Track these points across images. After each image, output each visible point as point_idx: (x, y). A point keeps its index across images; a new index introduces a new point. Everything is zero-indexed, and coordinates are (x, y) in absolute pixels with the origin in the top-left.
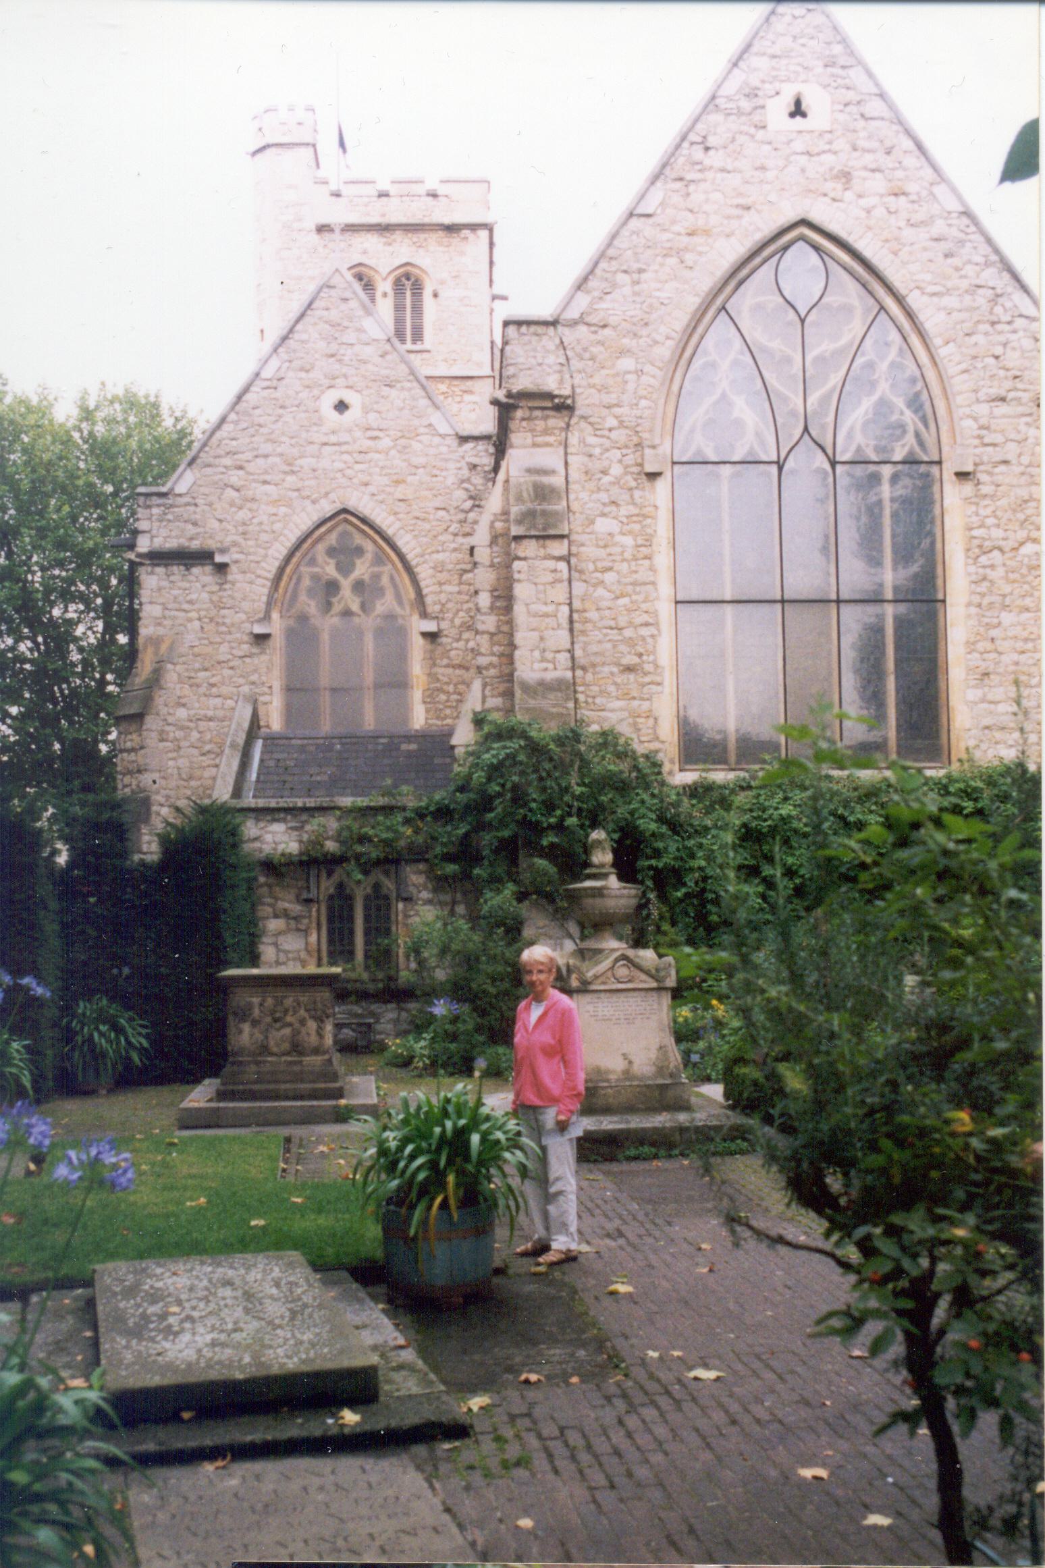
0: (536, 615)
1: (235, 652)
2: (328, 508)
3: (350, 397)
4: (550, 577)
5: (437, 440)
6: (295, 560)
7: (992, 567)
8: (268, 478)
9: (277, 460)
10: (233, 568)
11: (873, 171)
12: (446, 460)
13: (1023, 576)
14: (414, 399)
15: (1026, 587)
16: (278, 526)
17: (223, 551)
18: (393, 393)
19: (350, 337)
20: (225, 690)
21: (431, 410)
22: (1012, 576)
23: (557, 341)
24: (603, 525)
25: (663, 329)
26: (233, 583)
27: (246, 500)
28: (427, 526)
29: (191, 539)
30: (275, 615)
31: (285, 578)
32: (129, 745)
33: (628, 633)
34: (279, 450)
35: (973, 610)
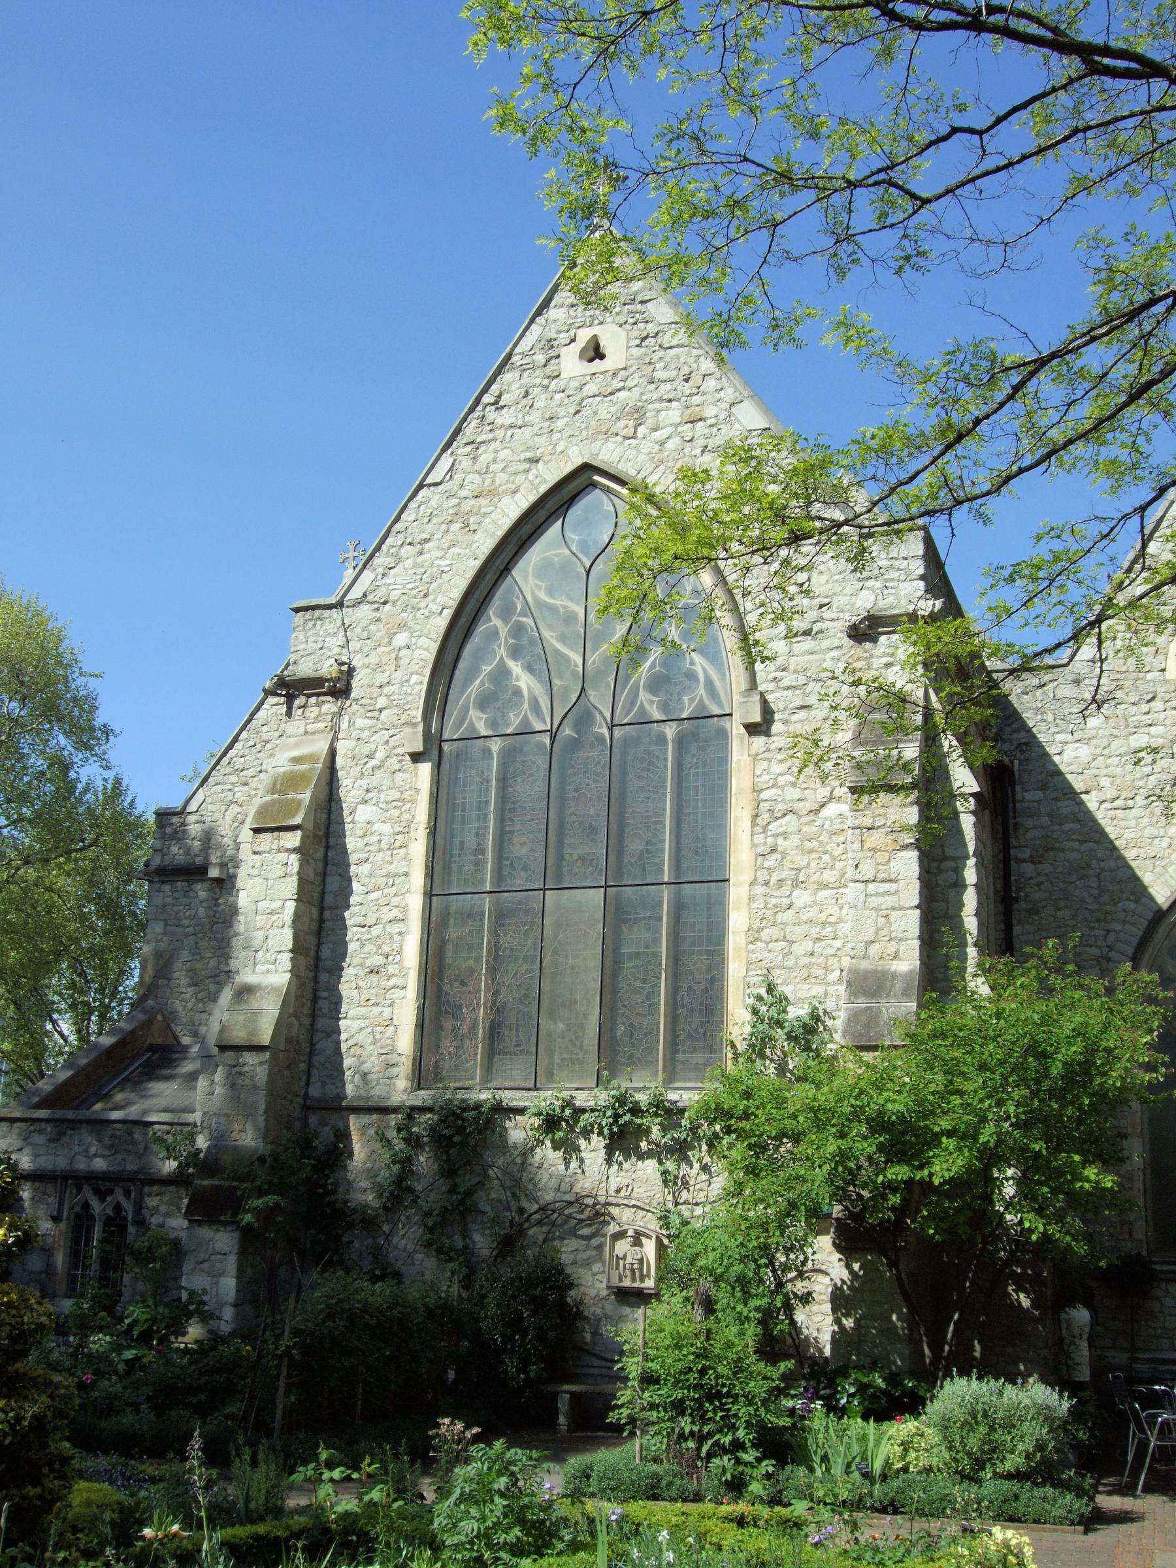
7: (785, 835)
11: (670, 401)
13: (821, 843)
15: (826, 857)
22: (808, 845)
23: (339, 623)
25: (441, 599)
35: (759, 889)
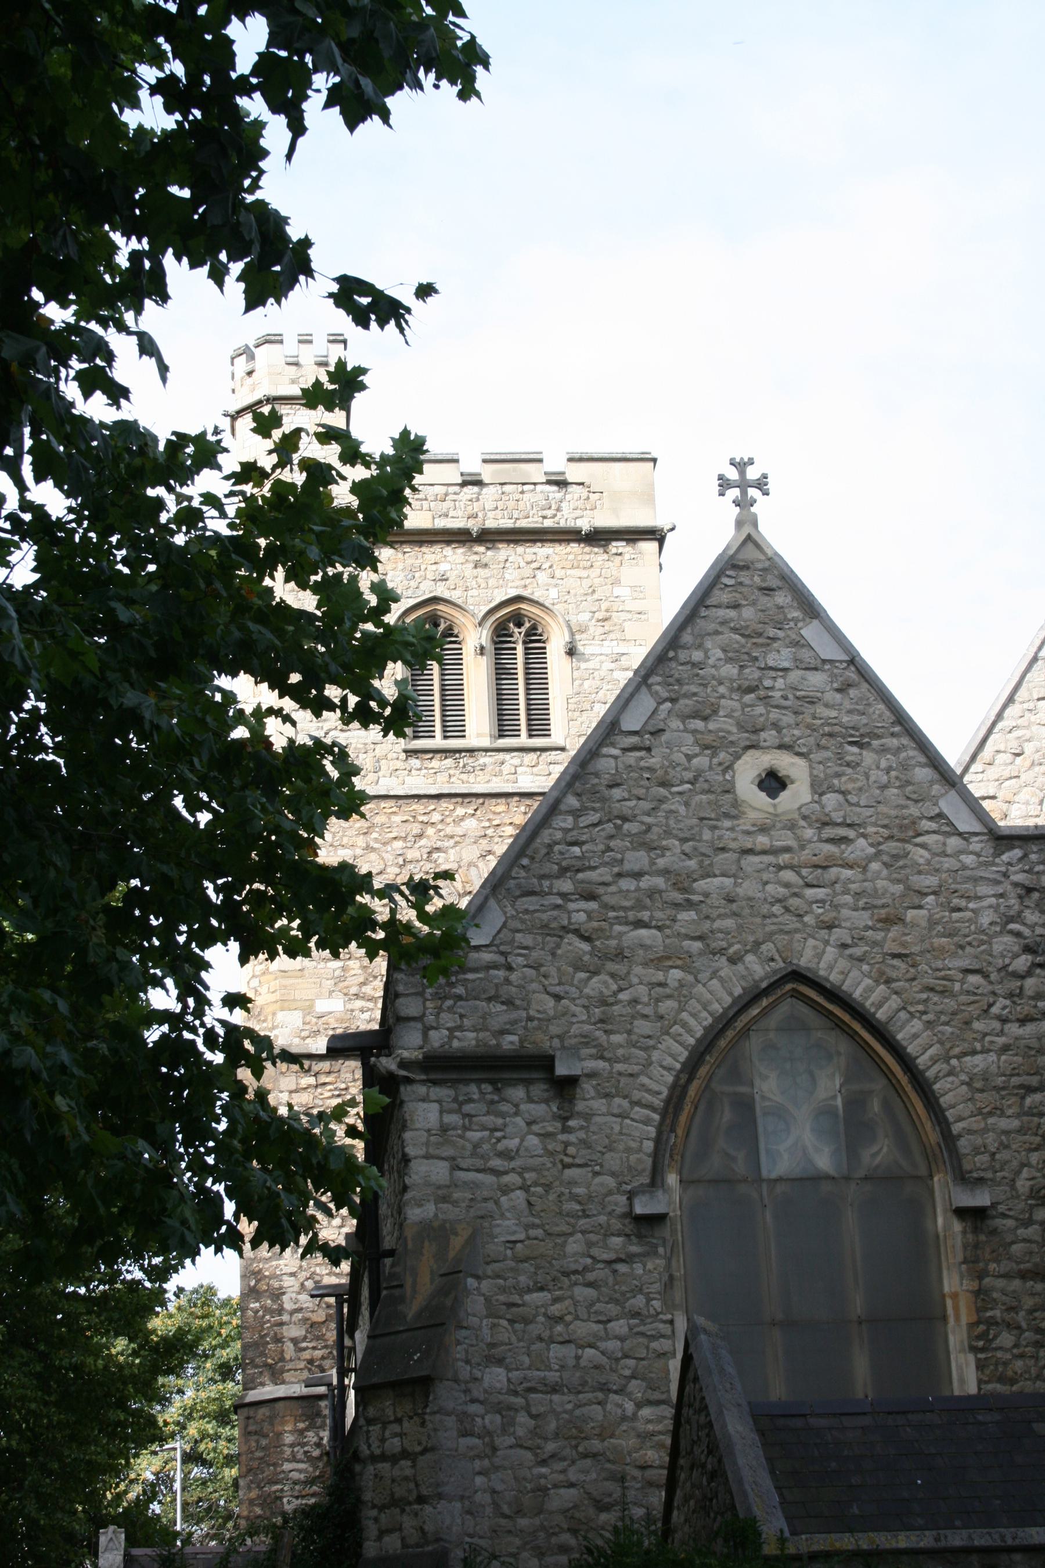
1: (595, 1251)
2: (756, 969)
3: (786, 763)
5: (954, 842)
6: (703, 1071)
8: (645, 915)
9: (660, 882)
10: (587, 1087)
12: (976, 880)
14: (905, 767)
16: (668, 1006)
17: (573, 1052)
18: (868, 757)
19: (782, 657)
20: (583, 1329)
21: (936, 789)
26: (588, 1116)
27: (606, 957)
28: (950, 1004)
29: (503, 1032)
30: (672, 1179)
31: (687, 1108)
32: (394, 1445)
34: (661, 862)
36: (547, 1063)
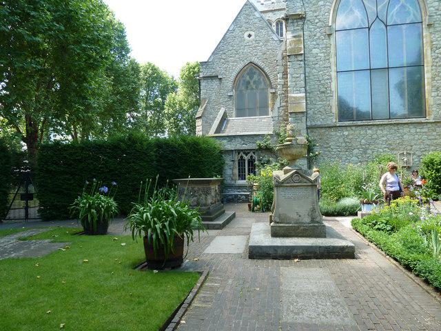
0: (294, 78)
3: (252, 33)
4: (298, 66)
24: (315, 51)
33: (322, 82)
35: (434, 68)
36: (217, 76)
